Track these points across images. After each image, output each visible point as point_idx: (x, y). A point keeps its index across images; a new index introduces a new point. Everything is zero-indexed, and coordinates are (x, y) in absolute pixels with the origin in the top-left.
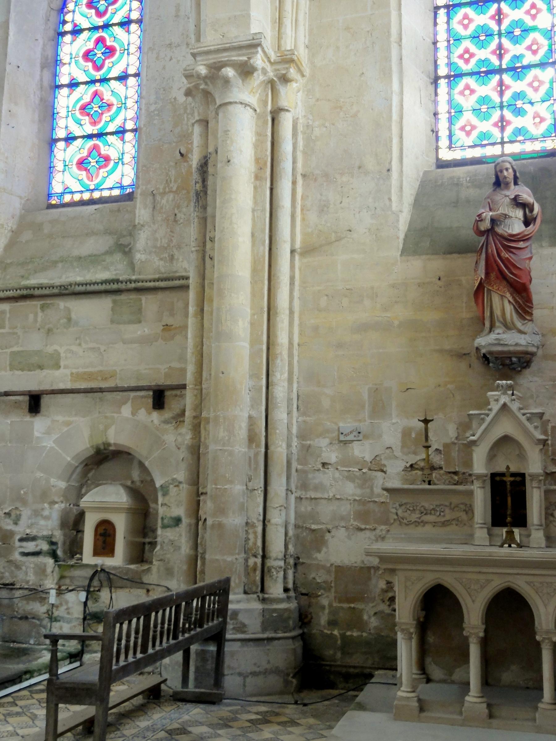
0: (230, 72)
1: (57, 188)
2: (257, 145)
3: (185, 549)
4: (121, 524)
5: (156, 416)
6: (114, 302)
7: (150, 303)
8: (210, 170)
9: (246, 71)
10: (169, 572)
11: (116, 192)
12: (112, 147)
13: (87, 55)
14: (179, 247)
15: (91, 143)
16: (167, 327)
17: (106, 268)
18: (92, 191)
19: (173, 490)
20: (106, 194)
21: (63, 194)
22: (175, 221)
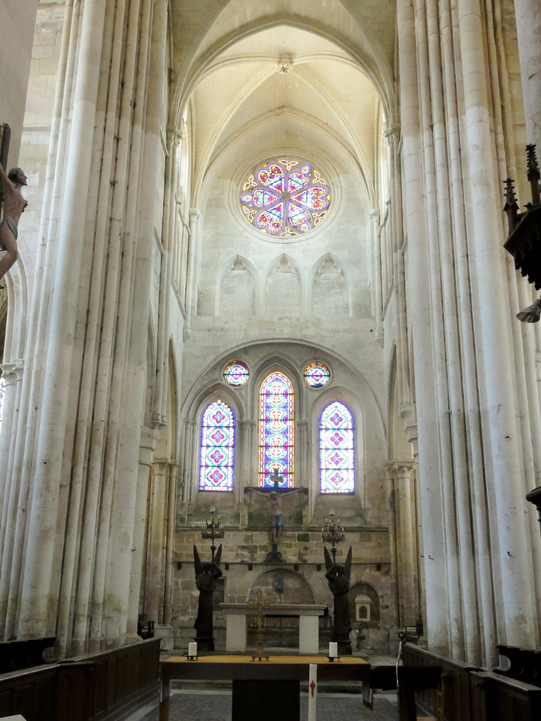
0: (406, 469)
1: (323, 487)
2: (411, 489)
3: (395, 614)
4: (368, 607)
5: (378, 573)
6: (361, 534)
7: (373, 536)
8: (396, 495)
9: (410, 468)
10: (386, 623)
11: (347, 491)
12: (344, 474)
13: (332, 439)
14: (382, 518)
15: (335, 472)
16: (379, 544)
17: (356, 523)
18: (337, 490)
19: (385, 597)
20: (343, 491)
21: (326, 489)
22: (380, 509)
